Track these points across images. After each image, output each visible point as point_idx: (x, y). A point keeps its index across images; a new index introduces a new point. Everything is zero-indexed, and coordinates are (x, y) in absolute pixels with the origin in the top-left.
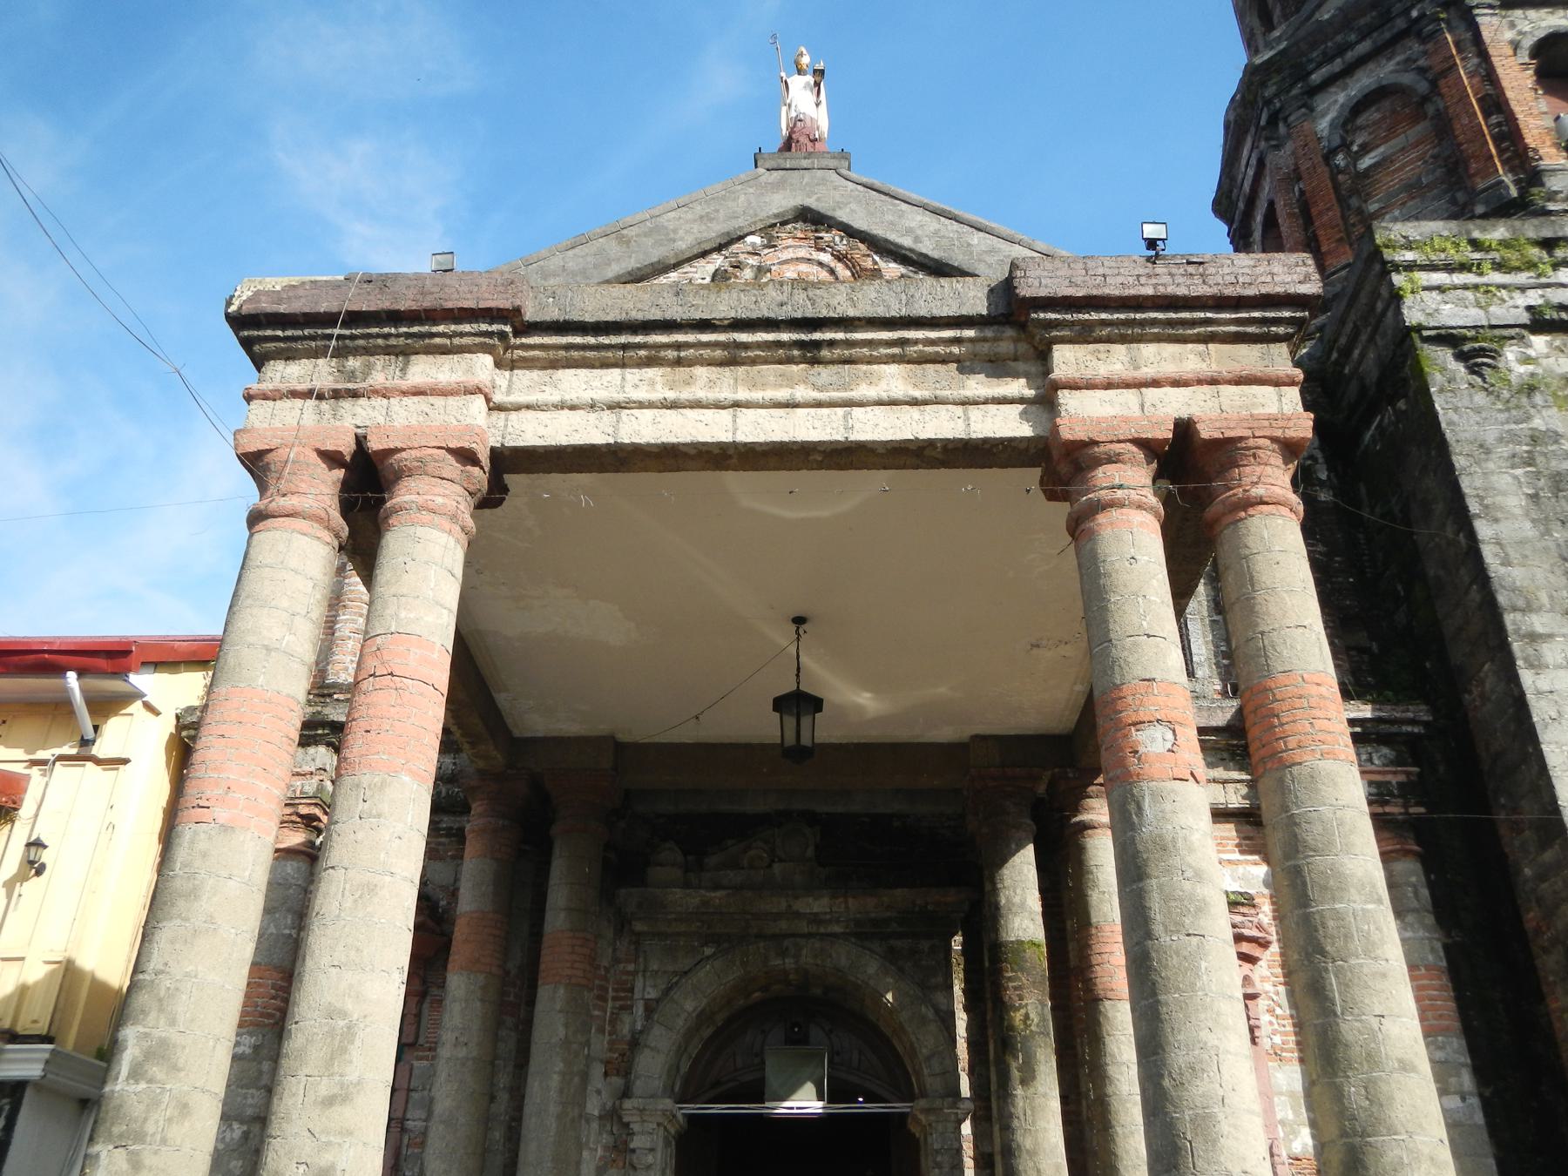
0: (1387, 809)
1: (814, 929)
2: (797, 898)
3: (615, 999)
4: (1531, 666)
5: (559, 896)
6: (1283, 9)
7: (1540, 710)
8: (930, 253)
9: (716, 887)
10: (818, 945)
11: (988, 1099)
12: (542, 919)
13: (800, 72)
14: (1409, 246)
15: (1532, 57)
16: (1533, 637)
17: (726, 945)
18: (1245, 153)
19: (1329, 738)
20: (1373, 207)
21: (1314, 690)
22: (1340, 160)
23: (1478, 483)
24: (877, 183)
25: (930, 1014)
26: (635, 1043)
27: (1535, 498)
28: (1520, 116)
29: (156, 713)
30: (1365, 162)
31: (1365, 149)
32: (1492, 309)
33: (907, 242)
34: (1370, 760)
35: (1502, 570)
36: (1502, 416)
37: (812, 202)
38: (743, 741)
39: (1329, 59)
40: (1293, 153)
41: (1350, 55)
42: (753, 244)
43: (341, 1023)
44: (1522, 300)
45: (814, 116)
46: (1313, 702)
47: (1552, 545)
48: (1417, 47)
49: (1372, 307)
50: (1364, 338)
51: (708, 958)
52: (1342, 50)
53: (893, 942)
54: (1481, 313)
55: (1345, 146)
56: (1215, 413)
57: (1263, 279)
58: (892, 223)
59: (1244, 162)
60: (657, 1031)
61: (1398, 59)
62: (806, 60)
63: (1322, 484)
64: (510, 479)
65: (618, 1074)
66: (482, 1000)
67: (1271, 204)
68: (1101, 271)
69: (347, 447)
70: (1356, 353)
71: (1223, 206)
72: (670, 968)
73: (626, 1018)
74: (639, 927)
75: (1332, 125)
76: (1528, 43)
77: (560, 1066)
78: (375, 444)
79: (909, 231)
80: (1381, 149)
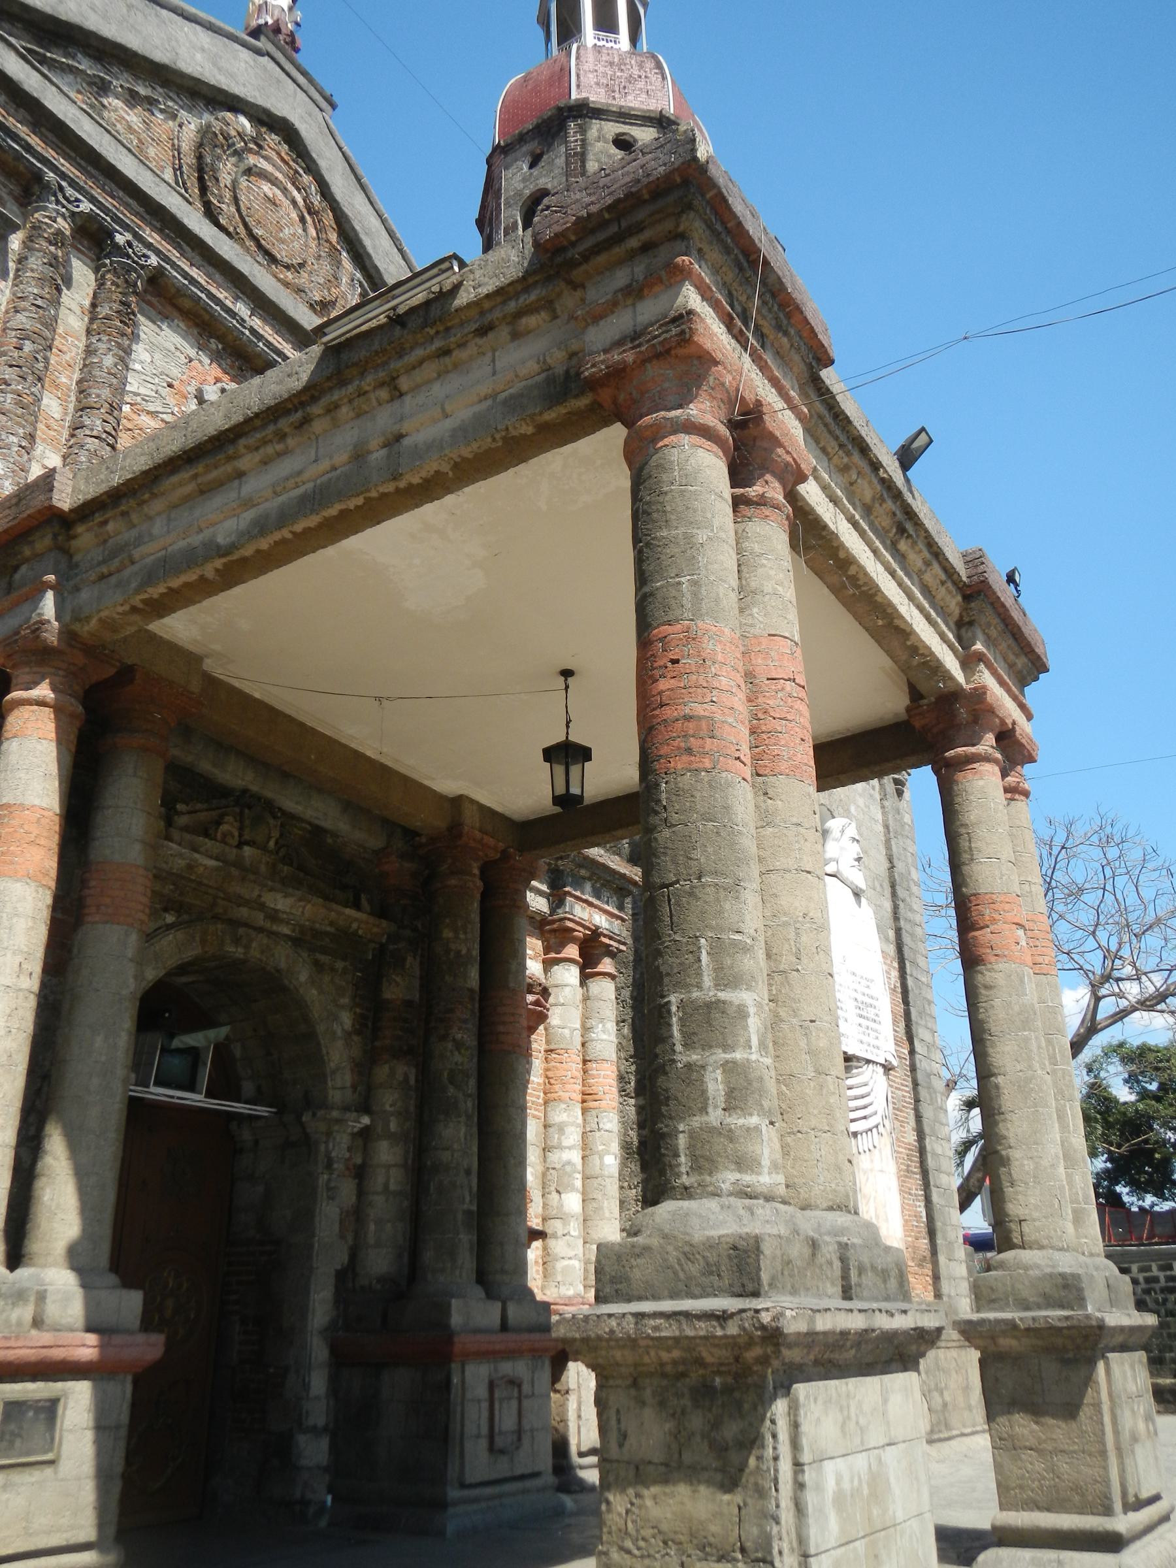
1: (268, 925)
2: (271, 890)
10: (265, 941)
17: (185, 917)
24: (353, 159)
33: (367, 242)
38: (302, 718)
42: (243, 126)
51: (169, 927)
53: (324, 959)
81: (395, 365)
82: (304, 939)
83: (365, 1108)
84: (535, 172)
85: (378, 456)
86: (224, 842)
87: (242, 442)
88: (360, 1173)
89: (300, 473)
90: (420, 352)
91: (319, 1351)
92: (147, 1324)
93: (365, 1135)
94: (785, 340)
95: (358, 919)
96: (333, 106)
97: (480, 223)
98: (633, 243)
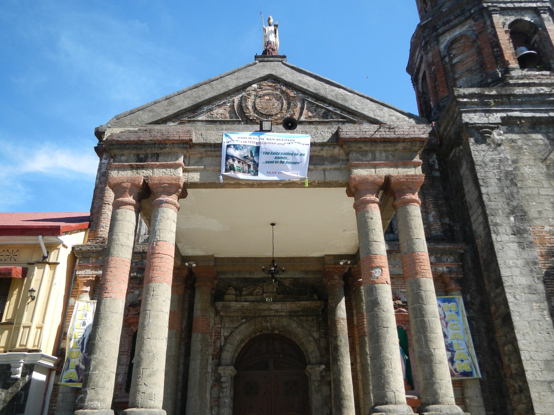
0: (452, 276)
1: (276, 314)
3: (215, 336)
4: (495, 233)
5: (198, 306)
6: (431, 4)
7: (497, 246)
8: (313, 91)
9: (246, 301)
10: (277, 319)
11: (329, 365)
12: (193, 311)
13: (270, 25)
14: (465, 96)
15: (509, 27)
16: (496, 224)
18: (417, 53)
19: (425, 271)
20: (457, 76)
21: (421, 257)
22: (447, 59)
23: (483, 175)
25: (312, 339)
26: (221, 349)
27: (499, 180)
28: (504, 49)
29: (66, 247)
30: (455, 61)
31: (455, 56)
32: (490, 118)
33: (305, 87)
34: (447, 260)
35: (488, 203)
36: (491, 153)
37: (273, 73)
39: (444, 24)
40: (432, 56)
41: (451, 24)
43: (152, 354)
44: (499, 115)
45: (274, 41)
46: (421, 261)
47: (504, 195)
48: (473, 23)
49: (453, 115)
50: (450, 124)
51: (244, 323)
52: (448, 22)
53: (301, 318)
54: (486, 119)
55: (449, 54)
56: (396, 174)
57: (411, 133)
58: (300, 80)
59: (416, 56)
60: (228, 346)
61: (466, 26)
62: (271, 21)
63: (437, 170)
64: (189, 191)
65: (216, 358)
66: (175, 338)
67: (425, 72)
68: (364, 130)
70: (448, 129)
71: (409, 69)
72: (232, 326)
73: (218, 342)
74: (222, 314)
75: (445, 48)
76: (508, 23)
77: (200, 357)
78: (150, 182)
79: (305, 84)
80: (460, 56)
82: (292, 315)
86: (257, 295)
94: (167, 149)
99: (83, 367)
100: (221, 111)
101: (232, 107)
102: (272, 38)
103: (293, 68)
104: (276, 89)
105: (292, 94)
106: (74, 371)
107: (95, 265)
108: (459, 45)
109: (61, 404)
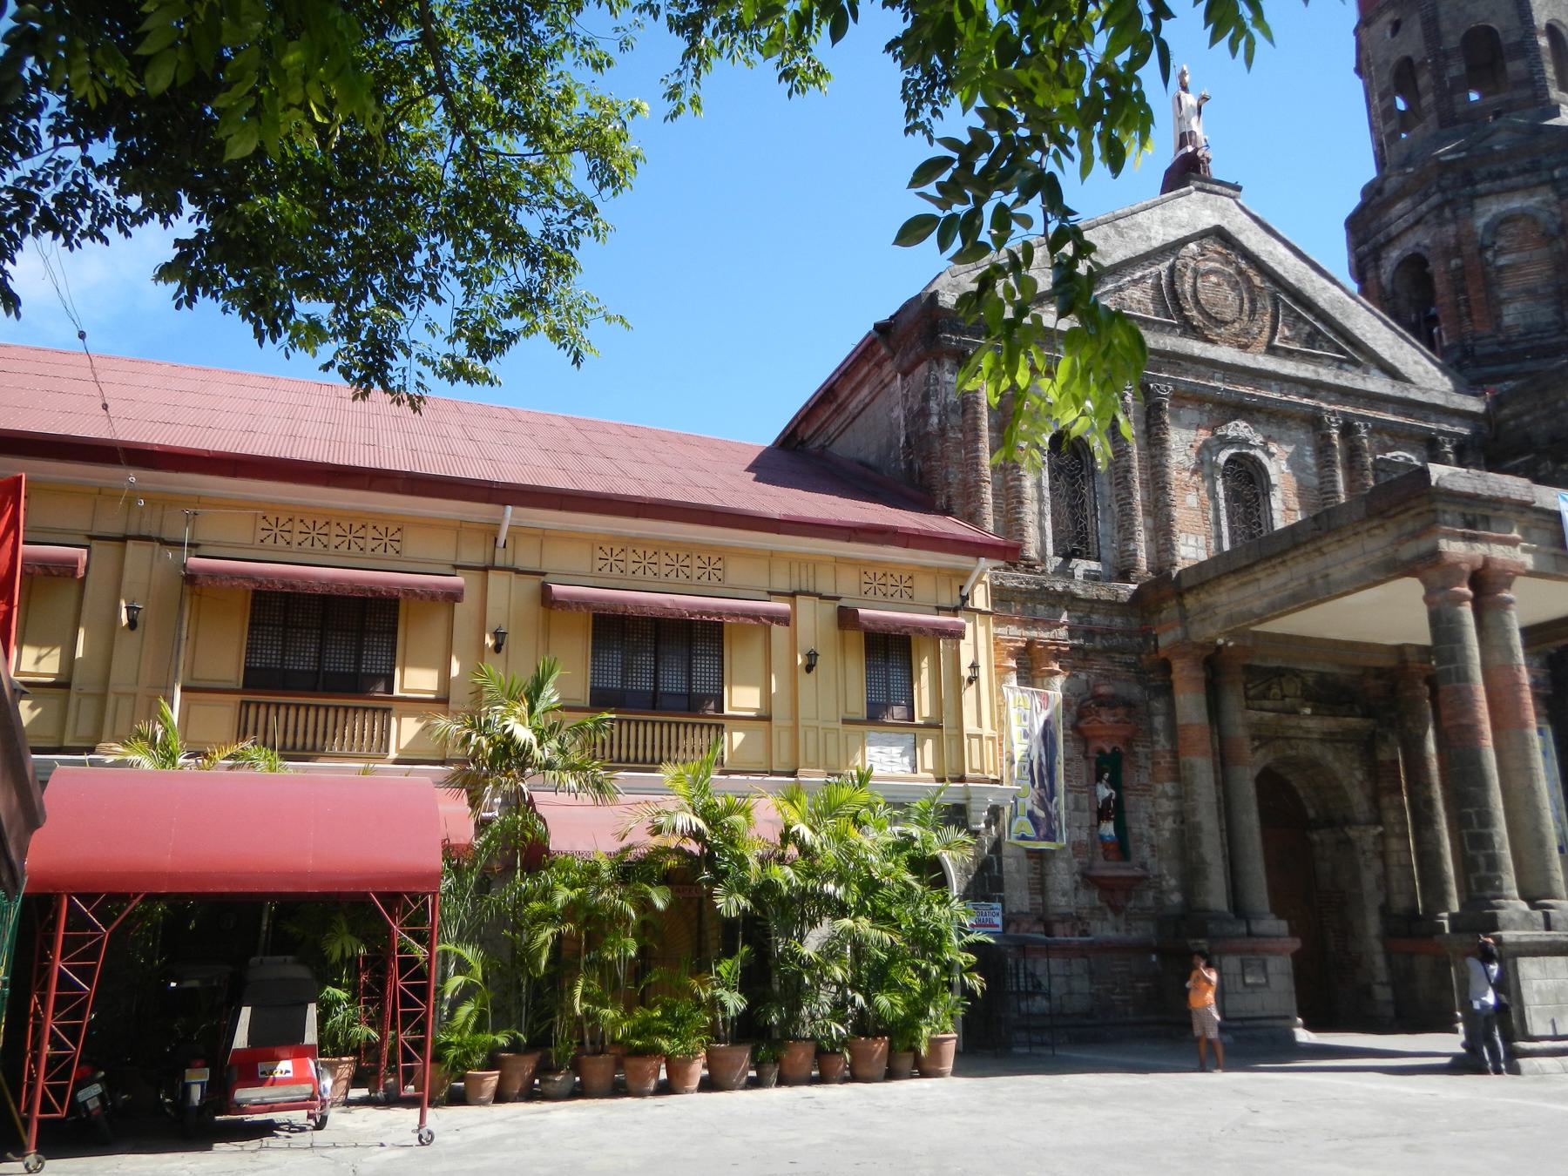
22: (1489, 255)
30: (1502, 261)
33: (1280, 270)
39: (1492, 177)
41: (1507, 182)
48: (1552, 196)
52: (1502, 175)
53: (1339, 745)
69: (1479, 564)
75: (1487, 225)
79: (1280, 263)
80: (1513, 256)
81: (1319, 544)
82: (1328, 738)
83: (1378, 821)
84: (1397, 39)
85: (1319, 582)
87: (1256, 568)
88: (1383, 855)
89: (1285, 584)
90: (1328, 540)
91: (1377, 946)
92: (1293, 933)
93: (1382, 836)
95: (1353, 722)
96: (1238, 188)
97: (1359, 71)
98: (1412, 512)
99: (1041, 814)
100: (1136, 293)
101: (1157, 287)
102: (1196, 126)
103: (1255, 219)
104: (1228, 263)
105: (1257, 281)
106: (1026, 819)
107: (1025, 618)
108: (1512, 230)
109: (1016, 876)
